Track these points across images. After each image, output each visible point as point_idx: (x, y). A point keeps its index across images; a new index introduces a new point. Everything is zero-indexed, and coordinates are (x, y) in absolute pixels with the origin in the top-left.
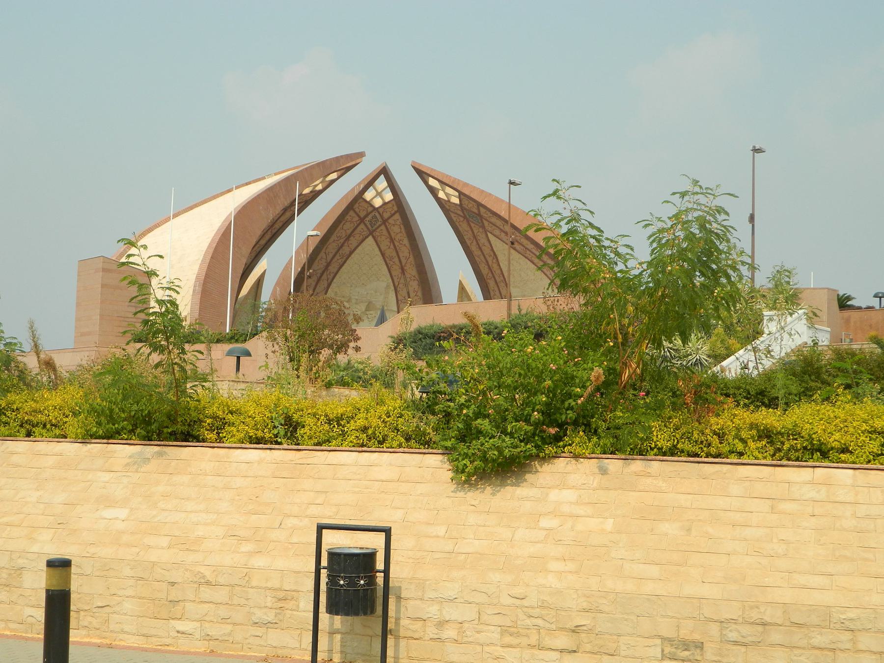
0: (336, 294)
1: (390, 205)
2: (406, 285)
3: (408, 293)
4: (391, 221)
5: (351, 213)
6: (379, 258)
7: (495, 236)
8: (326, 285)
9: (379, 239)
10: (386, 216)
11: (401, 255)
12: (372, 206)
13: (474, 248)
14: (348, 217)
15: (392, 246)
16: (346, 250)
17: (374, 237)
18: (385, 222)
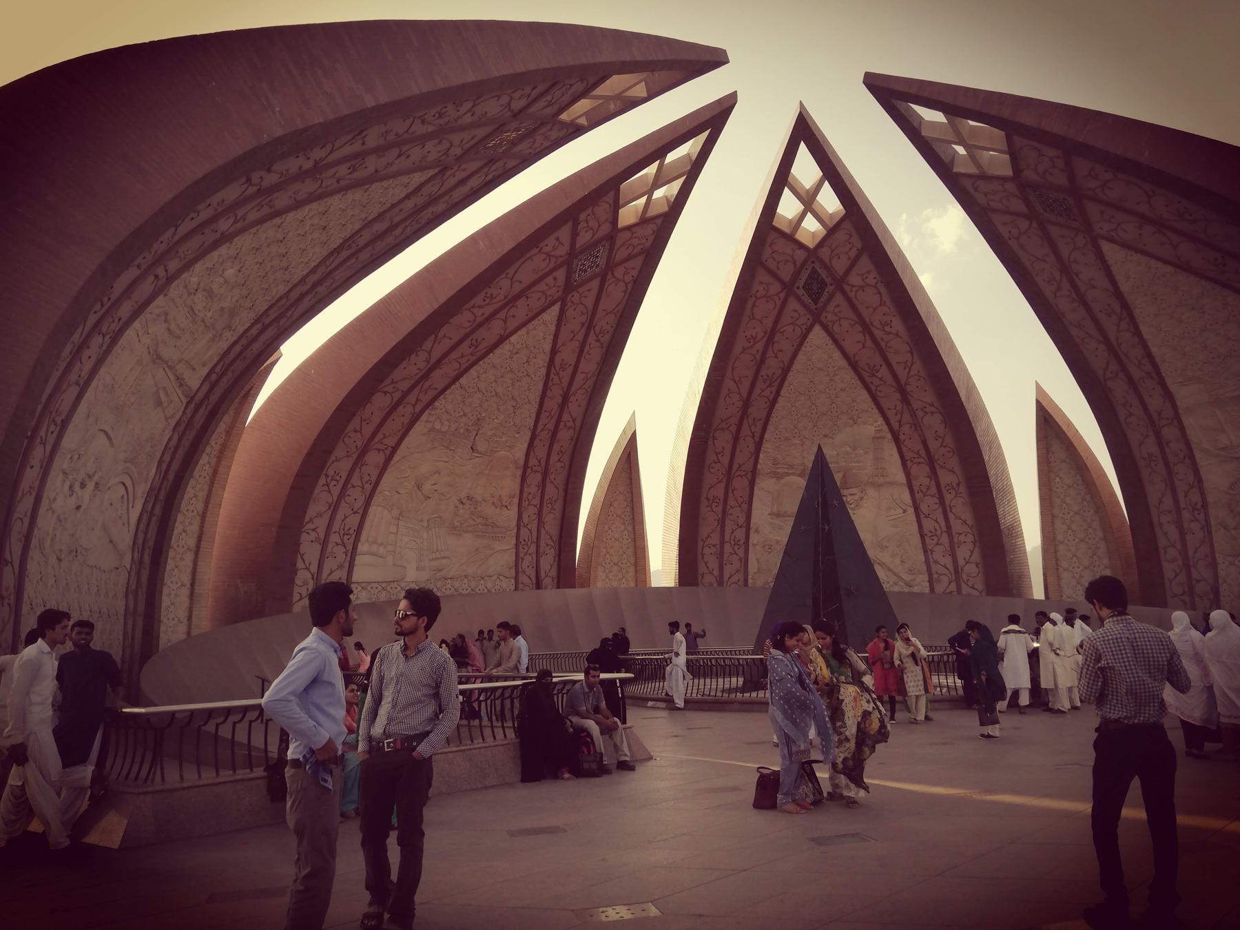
0: (775, 462)
1: (841, 235)
2: (917, 426)
3: (924, 443)
5: (762, 275)
6: (848, 376)
7: (1124, 245)
8: (752, 448)
9: (836, 329)
10: (840, 266)
11: (893, 360)
12: (801, 246)
13: (1064, 304)
15: (869, 343)
16: (772, 366)
17: (825, 328)
18: (840, 283)
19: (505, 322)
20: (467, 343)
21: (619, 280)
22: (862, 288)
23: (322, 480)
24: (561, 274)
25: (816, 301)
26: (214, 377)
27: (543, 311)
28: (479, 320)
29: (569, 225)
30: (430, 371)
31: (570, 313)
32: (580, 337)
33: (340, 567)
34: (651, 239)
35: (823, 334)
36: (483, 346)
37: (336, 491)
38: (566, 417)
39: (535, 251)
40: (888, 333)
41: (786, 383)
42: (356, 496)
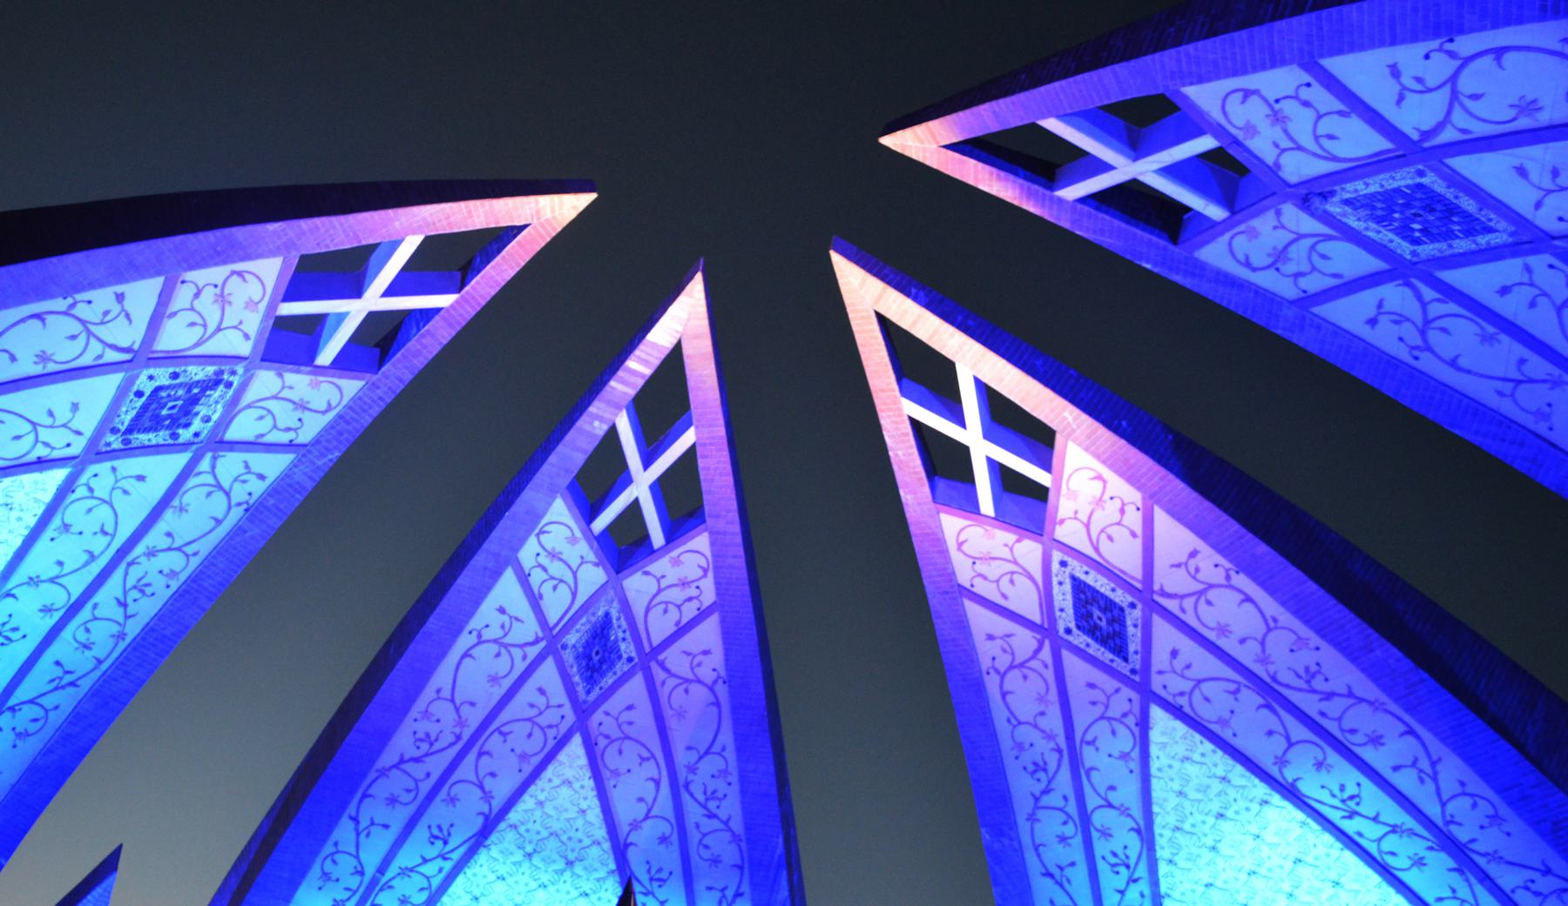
4: (1166, 578)
5: (980, 620)
10: (1125, 555)
14: (987, 652)
15: (1298, 731)
19: (481, 787)
21: (687, 681)
22: (1200, 593)
24: (548, 673)
25: (1121, 651)
27: (550, 757)
28: (425, 787)
29: (509, 577)
31: (611, 760)
32: (664, 805)
34: (708, 585)
35: (1180, 727)
40: (1329, 696)
41: (1163, 868)
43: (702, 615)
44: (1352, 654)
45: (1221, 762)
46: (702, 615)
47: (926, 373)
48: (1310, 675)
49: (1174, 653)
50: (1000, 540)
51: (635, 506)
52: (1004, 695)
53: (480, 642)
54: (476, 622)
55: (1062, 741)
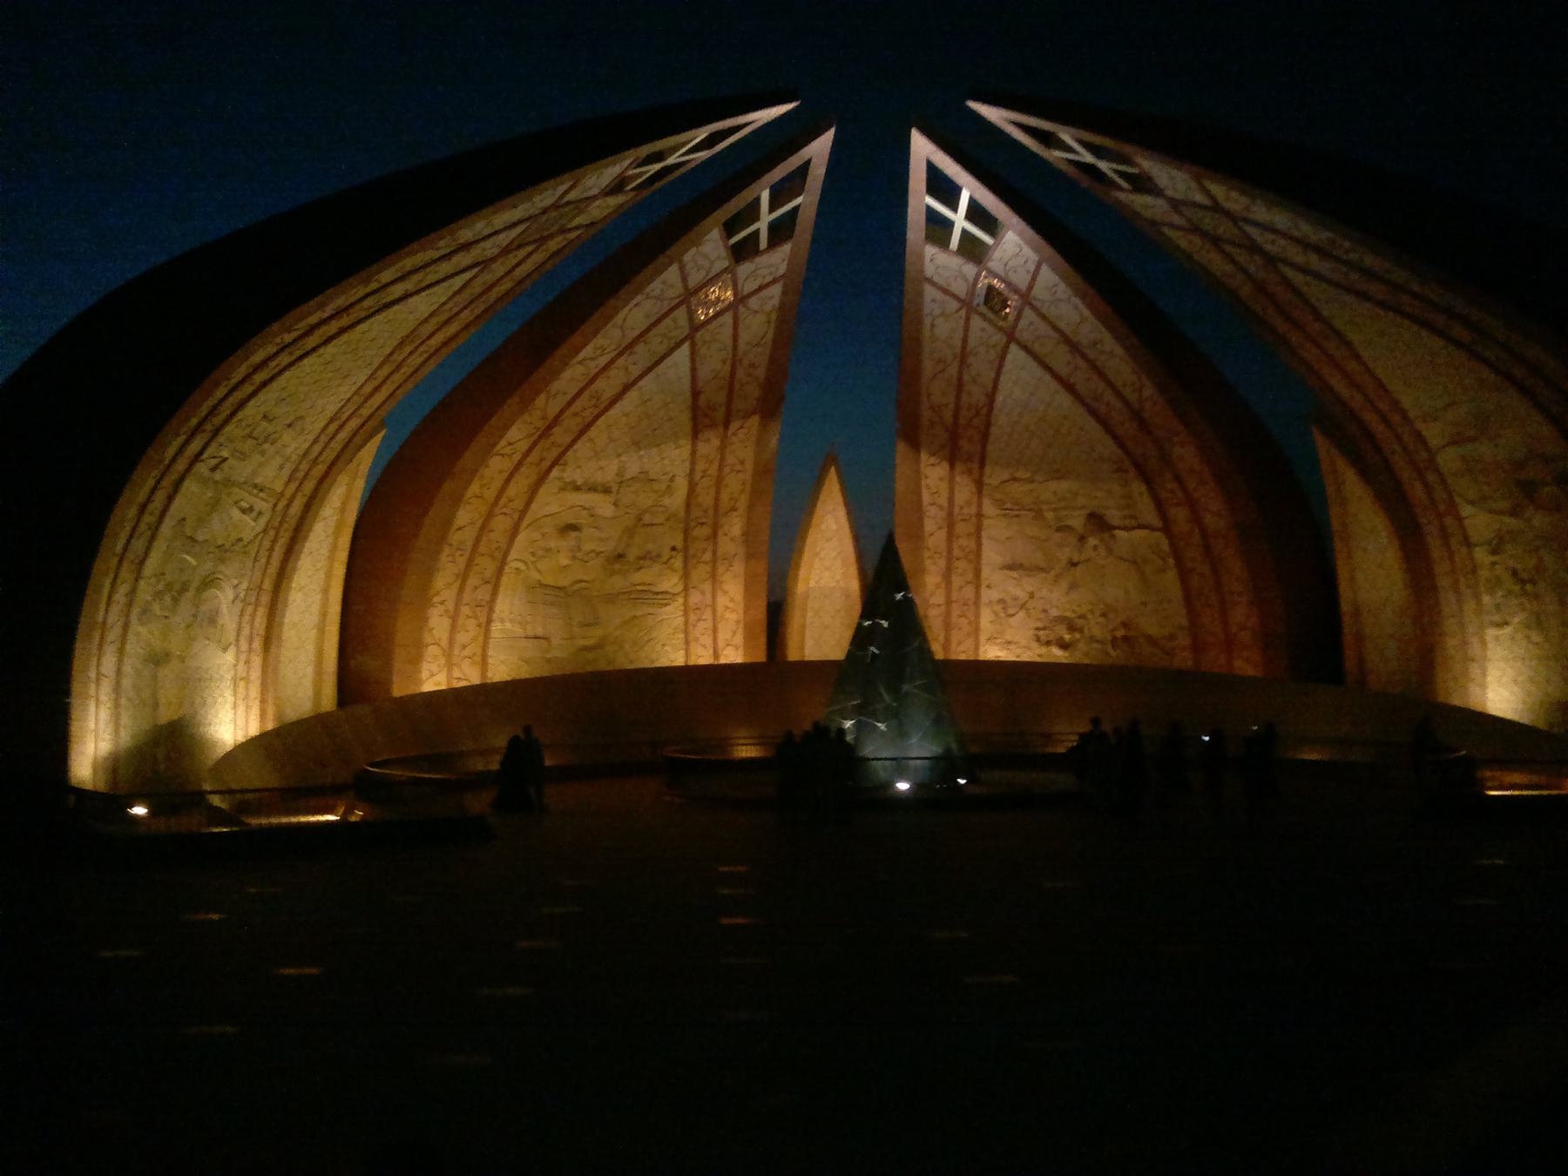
4: (1036, 292)
9: (1036, 347)
10: (1021, 281)
18: (1026, 297)
20: (586, 394)
23: (447, 550)
26: (300, 475)
29: (674, 268)
30: (550, 427)
31: (703, 351)
33: (475, 639)
35: (1022, 354)
36: (608, 394)
37: (462, 561)
38: (730, 459)
39: (639, 298)
40: (1102, 352)
41: (995, 412)
42: (486, 566)
43: (774, 281)
44: (1118, 338)
45: (1038, 371)
46: (774, 281)
47: (944, 189)
48: (1095, 344)
49: (1031, 323)
50: (955, 262)
51: (756, 233)
52: (933, 326)
53: (648, 297)
54: (648, 289)
55: (958, 350)
